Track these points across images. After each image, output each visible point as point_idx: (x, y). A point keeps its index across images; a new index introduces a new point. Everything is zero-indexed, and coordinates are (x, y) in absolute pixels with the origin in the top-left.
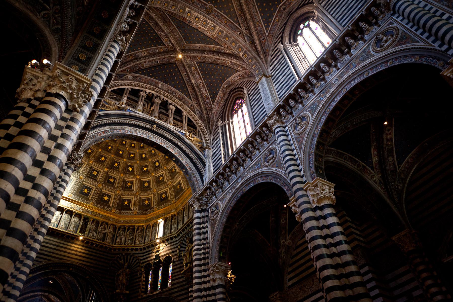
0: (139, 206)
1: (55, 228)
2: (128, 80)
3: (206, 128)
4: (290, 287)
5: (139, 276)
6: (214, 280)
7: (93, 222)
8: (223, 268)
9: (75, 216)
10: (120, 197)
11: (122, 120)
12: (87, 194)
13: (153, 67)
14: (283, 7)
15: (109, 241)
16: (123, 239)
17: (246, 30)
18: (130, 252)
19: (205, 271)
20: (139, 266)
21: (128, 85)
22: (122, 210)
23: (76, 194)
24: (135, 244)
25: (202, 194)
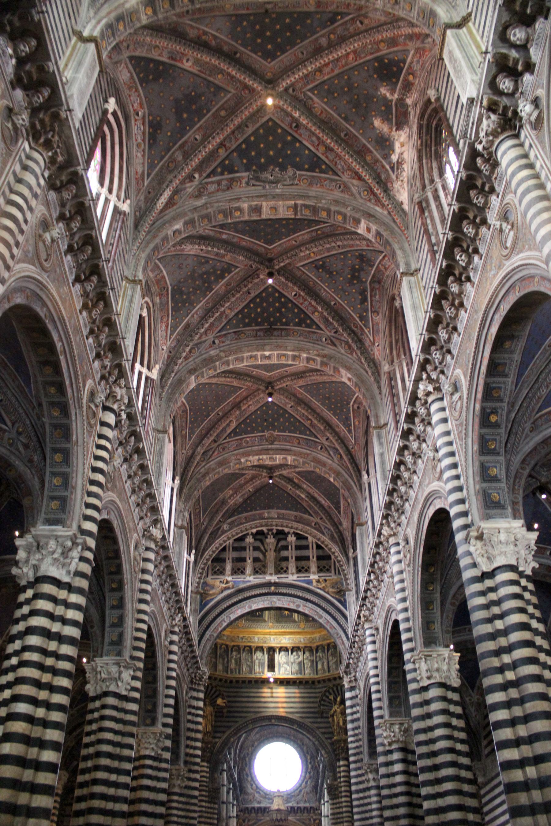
11: (234, 600)
16: (326, 664)
21: (229, 538)
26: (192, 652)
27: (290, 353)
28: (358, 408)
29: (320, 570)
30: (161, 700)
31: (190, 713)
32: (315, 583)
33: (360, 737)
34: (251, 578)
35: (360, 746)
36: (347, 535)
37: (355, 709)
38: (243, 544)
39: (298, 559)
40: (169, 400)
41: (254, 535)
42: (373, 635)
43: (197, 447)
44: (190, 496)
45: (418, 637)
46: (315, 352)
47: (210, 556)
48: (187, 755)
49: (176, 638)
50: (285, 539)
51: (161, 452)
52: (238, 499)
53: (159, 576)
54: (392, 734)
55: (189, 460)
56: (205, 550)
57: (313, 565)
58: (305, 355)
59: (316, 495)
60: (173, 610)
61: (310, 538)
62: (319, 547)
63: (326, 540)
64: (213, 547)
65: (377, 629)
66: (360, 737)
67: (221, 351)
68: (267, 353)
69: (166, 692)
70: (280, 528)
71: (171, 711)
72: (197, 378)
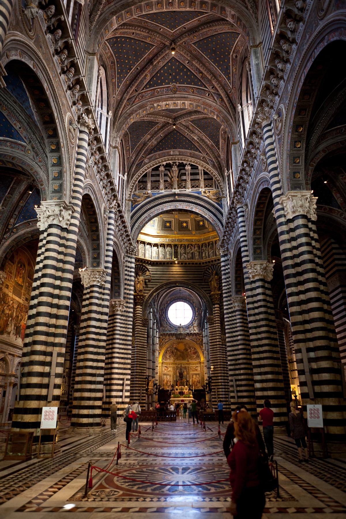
1: (157, 260)
2: (147, 164)
3: (220, 176)
9: (167, 246)
10: (195, 220)
11: (152, 204)
12: (170, 227)
16: (207, 253)
18: (214, 263)
21: (148, 168)
22: (200, 230)
23: (162, 230)
24: (216, 256)
26: (126, 231)
28: (236, 57)
29: (206, 186)
30: (103, 252)
31: (126, 270)
33: (230, 283)
34: (163, 191)
35: (230, 288)
36: (224, 163)
37: (227, 267)
38: (157, 173)
39: (191, 180)
40: (97, 33)
42: (243, 212)
43: (124, 94)
44: (121, 128)
45: (286, 185)
47: (137, 179)
48: (125, 293)
49: (112, 215)
50: (184, 169)
51: (91, 68)
52: (154, 142)
53: (95, 163)
54: (256, 271)
55: (119, 103)
56: (133, 175)
57: (202, 184)
59: (204, 138)
60: (110, 196)
61: (200, 168)
62: (205, 173)
63: (210, 167)
64: (138, 173)
65: (246, 205)
66: (230, 283)
69: (106, 248)
70: (181, 162)
71: (111, 259)
72: (118, 18)
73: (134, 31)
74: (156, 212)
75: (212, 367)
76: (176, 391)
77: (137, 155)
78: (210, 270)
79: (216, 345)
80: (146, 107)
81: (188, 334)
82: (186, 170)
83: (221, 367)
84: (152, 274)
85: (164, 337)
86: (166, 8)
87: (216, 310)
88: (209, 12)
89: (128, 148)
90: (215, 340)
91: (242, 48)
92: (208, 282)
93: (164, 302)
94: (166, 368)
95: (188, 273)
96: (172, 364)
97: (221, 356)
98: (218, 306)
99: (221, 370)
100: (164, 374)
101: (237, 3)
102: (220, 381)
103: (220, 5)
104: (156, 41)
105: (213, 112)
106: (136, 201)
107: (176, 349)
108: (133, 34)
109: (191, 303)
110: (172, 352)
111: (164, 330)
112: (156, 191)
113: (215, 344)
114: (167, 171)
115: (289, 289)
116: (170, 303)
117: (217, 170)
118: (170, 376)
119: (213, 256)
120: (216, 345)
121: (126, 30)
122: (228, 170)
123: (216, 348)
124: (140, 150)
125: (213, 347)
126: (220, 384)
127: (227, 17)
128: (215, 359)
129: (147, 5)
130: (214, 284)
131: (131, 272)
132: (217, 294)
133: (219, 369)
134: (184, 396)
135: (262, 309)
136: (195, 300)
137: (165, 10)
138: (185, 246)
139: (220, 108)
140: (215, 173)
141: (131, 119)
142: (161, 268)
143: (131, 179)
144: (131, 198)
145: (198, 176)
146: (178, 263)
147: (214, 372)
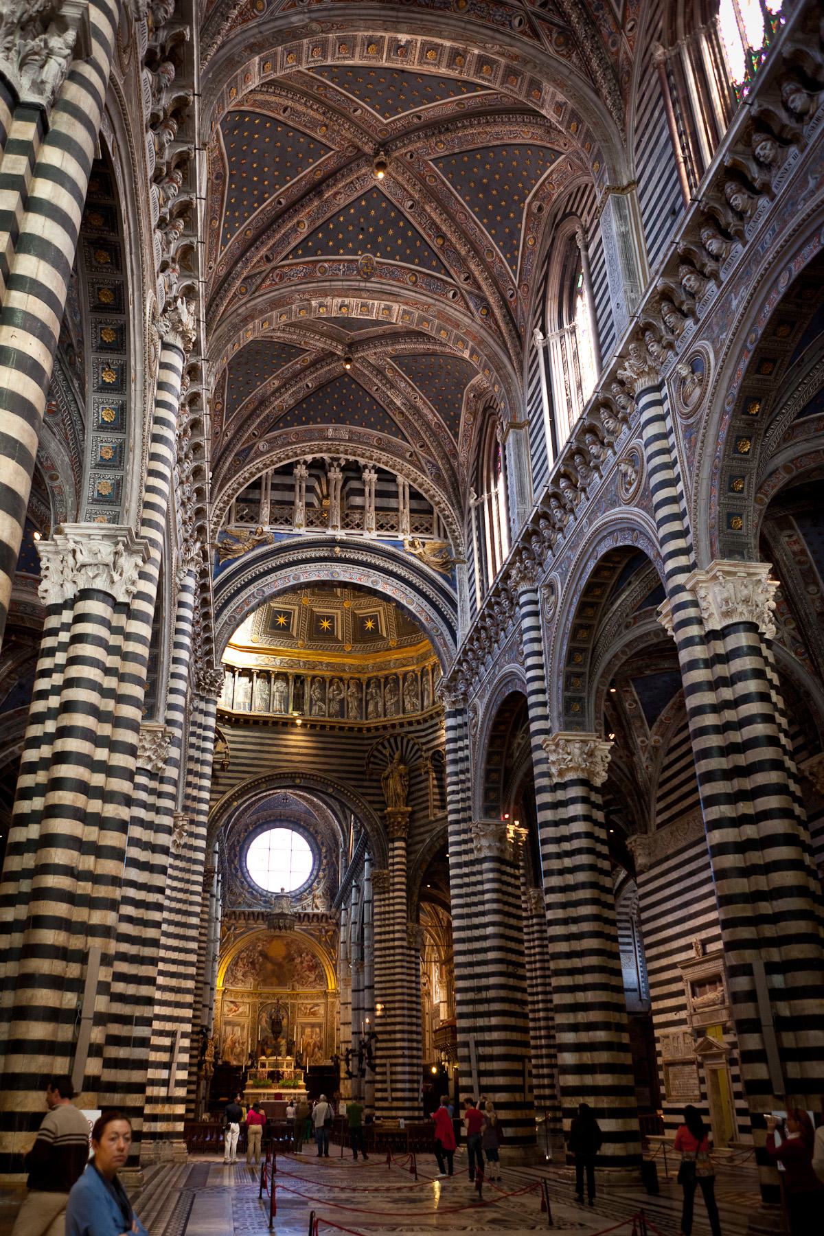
0: (397, 626)
1: (247, 712)
2: (263, 454)
3: (453, 505)
4: (659, 826)
5: (423, 777)
6: (479, 850)
7: (312, 683)
8: (492, 827)
9: (277, 678)
11: (272, 563)
12: (286, 628)
13: (303, 400)
14: (536, 204)
15: (353, 713)
17: (466, 279)
18: (398, 730)
19: (465, 831)
20: (421, 756)
21: (266, 466)
22: (365, 642)
23: (265, 633)
24: (404, 712)
25: (453, 678)
27: (448, 44)
31: (193, 734)
32: (407, 547)
38: (287, 480)
39: (377, 509)
41: (310, 466)
43: (236, 263)
46: (497, 48)
47: (235, 490)
50: (360, 479)
56: (226, 480)
58: (476, 52)
62: (415, 495)
63: (427, 481)
67: (312, 20)
68: (403, 38)
70: (351, 458)
73: (290, 103)
74: (280, 585)
75: (379, 1006)
76: (261, 1069)
77: (240, 429)
78: (385, 748)
79: (393, 948)
80: (288, 304)
81: (300, 917)
82: (364, 483)
83: (403, 1008)
84: (233, 749)
85: (232, 921)
86: (388, 58)
87: (398, 856)
88: (494, 85)
89: (219, 406)
90: (391, 936)
91: (562, 189)
92: (378, 781)
93: (239, 827)
94: (232, 1006)
95: (329, 753)
96: (250, 994)
97: (404, 977)
98: (402, 844)
99: (403, 1016)
100: (227, 1023)
101: (572, 77)
102: (398, 1044)
103: (528, 74)
104: (338, 139)
105: (463, 341)
106: (228, 550)
107: (263, 954)
108: (284, 111)
109: (311, 834)
110: (252, 963)
111: (233, 904)
112: (285, 529)
113: (391, 944)
114: (313, 479)
115: (715, 809)
116: (255, 829)
117: (445, 489)
118: (243, 1029)
119: (397, 712)
120: (393, 948)
121: (267, 98)
122: (479, 493)
123: (393, 955)
124: (249, 417)
125: (383, 953)
126: (399, 1052)
127: (542, 107)
128: (388, 985)
129: (342, 42)
130: (395, 786)
131: (205, 739)
132: (402, 814)
133: (398, 1012)
134: (281, 1082)
135: (583, 859)
136: (322, 827)
137: (384, 63)
138: (324, 681)
139: (481, 330)
140: (439, 496)
141: (247, 331)
142: (257, 734)
143: (220, 490)
144: (216, 542)
145: (392, 500)
146: (304, 725)
147: (383, 1021)
